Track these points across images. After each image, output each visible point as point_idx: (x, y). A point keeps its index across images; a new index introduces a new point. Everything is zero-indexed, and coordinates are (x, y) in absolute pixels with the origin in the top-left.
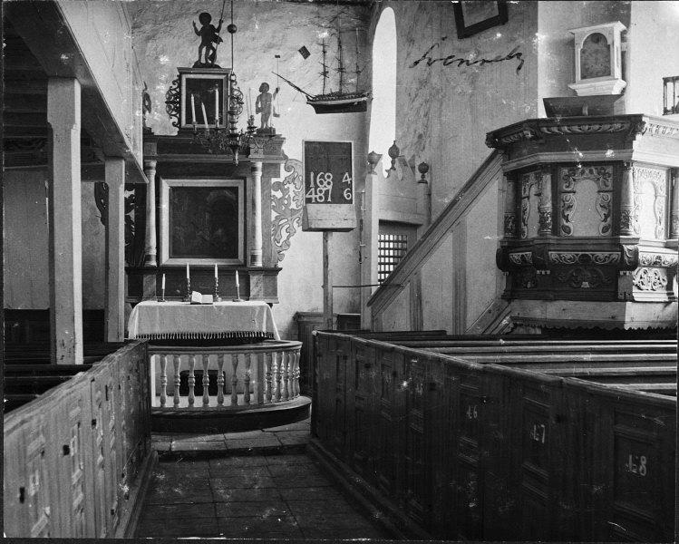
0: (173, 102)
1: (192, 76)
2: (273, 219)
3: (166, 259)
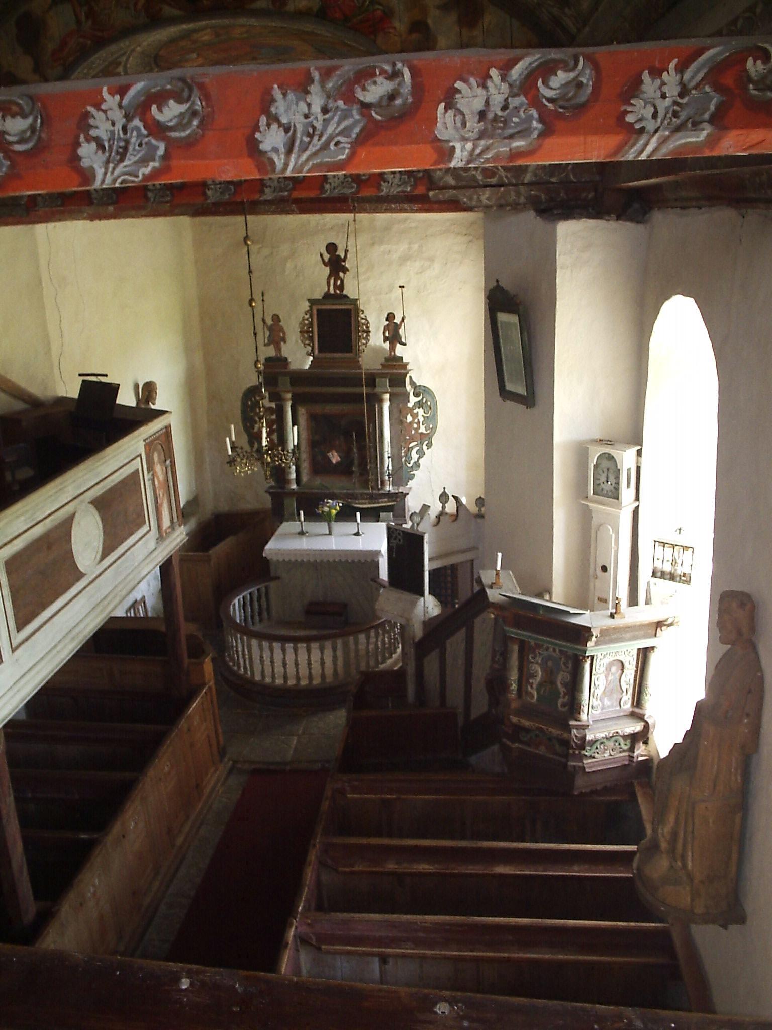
0: (307, 332)
1: (320, 307)
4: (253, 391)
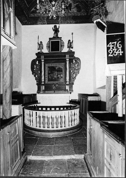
3: (47, 82)
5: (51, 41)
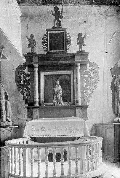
0: (45, 43)
2: (85, 86)
4: (22, 67)
5: (49, 32)
